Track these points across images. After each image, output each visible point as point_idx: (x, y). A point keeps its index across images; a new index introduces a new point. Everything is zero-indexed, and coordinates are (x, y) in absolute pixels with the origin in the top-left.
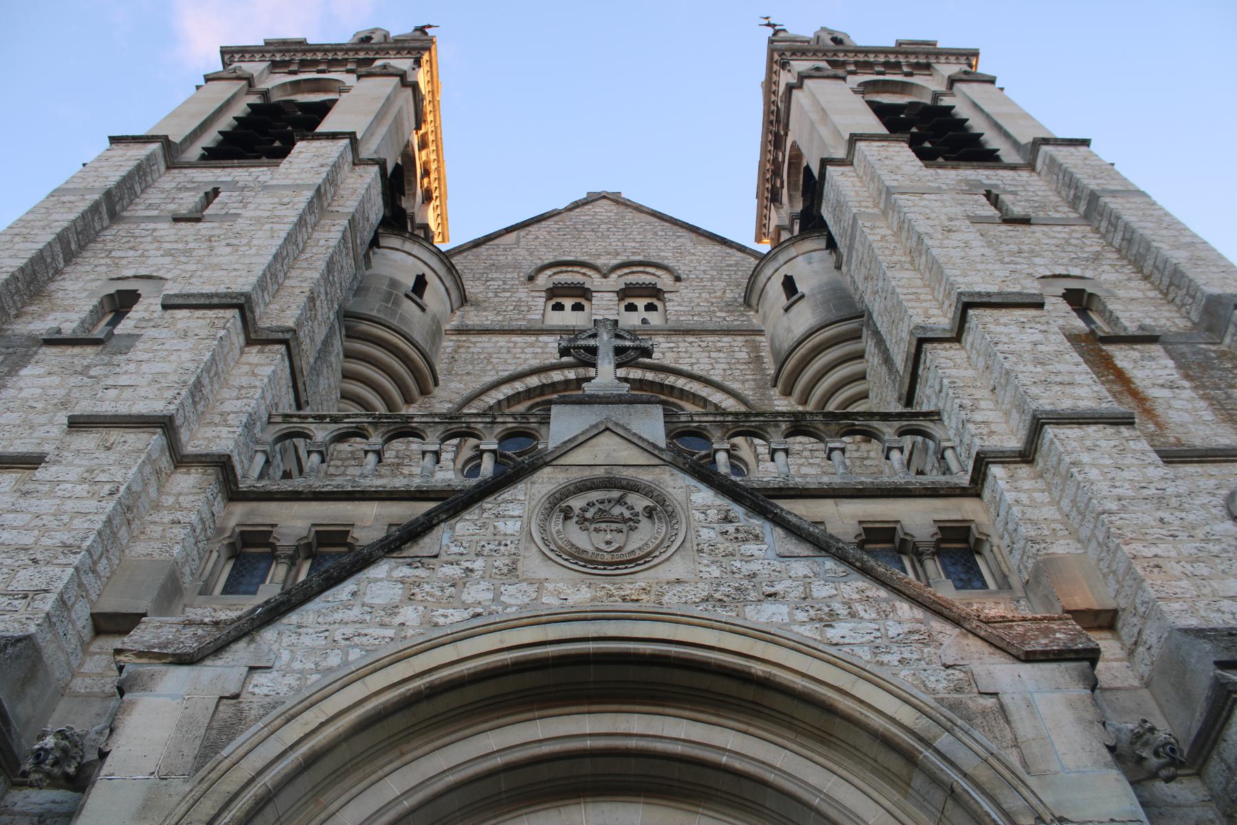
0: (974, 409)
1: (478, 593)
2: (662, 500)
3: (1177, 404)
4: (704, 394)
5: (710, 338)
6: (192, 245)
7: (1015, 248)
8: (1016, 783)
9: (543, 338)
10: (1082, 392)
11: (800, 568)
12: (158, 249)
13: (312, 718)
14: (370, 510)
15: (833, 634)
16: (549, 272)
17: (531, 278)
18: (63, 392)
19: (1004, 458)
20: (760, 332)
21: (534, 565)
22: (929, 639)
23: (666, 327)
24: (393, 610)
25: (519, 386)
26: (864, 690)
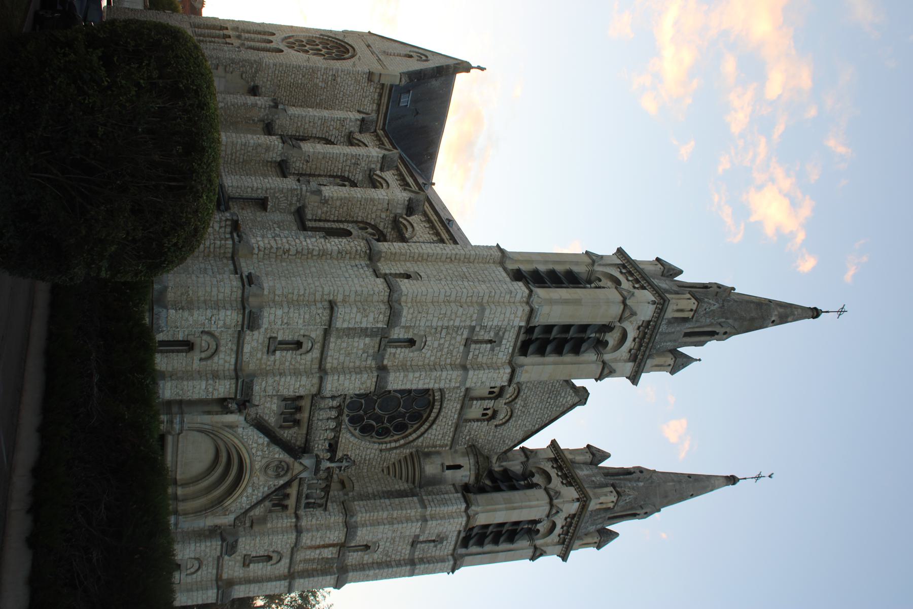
1: (259, 453)
2: (282, 476)
5: (451, 435)
6: (445, 350)
7: (397, 539)
10: (308, 541)
11: (260, 495)
12: (445, 341)
14: (306, 415)
15: (244, 498)
20: (451, 448)
21: (264, 461)
24: (256, 443)
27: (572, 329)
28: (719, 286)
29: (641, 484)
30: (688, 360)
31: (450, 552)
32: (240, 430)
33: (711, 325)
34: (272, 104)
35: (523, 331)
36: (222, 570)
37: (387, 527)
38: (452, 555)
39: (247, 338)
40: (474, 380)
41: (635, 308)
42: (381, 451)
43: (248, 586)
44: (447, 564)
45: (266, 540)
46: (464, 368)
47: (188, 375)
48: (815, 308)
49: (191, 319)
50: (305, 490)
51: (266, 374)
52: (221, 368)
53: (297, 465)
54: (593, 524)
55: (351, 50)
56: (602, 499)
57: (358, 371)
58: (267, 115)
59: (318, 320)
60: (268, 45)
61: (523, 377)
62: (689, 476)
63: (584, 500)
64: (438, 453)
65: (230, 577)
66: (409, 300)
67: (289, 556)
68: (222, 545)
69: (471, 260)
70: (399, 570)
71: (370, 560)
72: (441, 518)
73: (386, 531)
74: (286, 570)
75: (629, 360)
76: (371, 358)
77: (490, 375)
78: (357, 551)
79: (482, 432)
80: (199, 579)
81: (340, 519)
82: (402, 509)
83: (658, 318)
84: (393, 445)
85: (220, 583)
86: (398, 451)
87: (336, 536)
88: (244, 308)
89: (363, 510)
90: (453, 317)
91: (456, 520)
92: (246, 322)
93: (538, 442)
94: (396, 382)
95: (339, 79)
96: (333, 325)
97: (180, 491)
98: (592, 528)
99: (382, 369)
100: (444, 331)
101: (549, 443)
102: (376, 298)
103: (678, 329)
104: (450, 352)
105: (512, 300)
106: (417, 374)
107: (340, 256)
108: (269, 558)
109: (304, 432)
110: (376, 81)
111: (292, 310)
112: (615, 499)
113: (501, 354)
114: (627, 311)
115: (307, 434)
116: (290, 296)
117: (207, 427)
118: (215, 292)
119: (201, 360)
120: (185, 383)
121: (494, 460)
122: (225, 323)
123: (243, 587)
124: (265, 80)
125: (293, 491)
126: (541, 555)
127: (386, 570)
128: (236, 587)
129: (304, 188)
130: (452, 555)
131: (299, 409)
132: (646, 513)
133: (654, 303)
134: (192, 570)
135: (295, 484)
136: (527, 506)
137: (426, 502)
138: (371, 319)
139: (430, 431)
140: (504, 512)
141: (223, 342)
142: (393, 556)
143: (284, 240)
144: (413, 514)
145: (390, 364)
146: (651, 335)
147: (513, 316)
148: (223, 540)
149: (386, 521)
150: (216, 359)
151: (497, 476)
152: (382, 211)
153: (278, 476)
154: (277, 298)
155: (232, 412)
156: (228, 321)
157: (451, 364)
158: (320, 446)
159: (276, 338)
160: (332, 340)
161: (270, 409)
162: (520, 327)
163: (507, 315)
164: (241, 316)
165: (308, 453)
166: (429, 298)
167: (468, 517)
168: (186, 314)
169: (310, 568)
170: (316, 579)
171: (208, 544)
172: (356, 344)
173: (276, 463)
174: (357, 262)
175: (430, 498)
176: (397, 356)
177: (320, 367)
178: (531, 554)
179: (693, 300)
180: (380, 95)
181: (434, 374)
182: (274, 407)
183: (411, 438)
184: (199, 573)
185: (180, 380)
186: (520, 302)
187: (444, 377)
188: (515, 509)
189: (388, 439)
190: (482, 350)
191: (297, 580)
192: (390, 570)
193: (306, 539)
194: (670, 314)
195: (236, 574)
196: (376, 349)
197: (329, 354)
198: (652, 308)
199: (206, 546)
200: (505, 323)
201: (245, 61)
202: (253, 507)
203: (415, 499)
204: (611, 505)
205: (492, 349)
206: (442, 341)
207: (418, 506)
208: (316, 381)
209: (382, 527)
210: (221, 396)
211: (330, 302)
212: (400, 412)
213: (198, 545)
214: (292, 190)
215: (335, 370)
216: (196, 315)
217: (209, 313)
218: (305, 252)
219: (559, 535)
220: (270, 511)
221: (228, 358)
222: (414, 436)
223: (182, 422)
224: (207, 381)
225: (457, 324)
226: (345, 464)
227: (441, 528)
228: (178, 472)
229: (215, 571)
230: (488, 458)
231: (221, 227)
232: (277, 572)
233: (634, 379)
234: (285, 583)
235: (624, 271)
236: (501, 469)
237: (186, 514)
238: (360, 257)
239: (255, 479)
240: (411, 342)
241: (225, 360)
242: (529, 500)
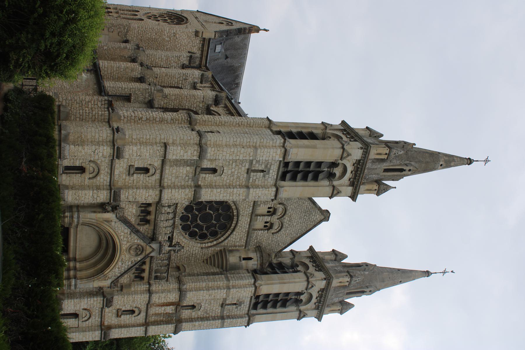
0: (162, 287)
1: (125, 239)
2: (139, 255)
3: (160, 310)
5: (245, 239)
6: (236, 176)
7: (212, 302)
8: (97, 279)
9: (251, 208)
10: (157, 300)
11: (126, 267)
13: (109, 228)
15: (117, 269)
17: (280, 204)
18: (181, 175)
19: (149, 287)
20: (245, 248)
21: (128, 244)
22: (115, 276)
23: (251, 230)
26: (109, 270)
27: (312, 164)
28: (405, 143)
29: (367, 273)
30: (387, 188)
31: (246, 312)
32: (113, 223)
33: (400, 165)
34: (136, 47)
35: (282, 165)
36: (104, 319)
37: (205, 292)
38: (248, 314)
39: (117, 165)
40: (254, 195)
41: (350, 151)
42: (202, 248)
43: (120, 329)
44: (244, 319)
45: (131, 298)
46: (248, 187)
47: (82, 187)
48: (469, 159)
49: (83, 151)
50: (154, 267)
51: (128, 187)
52: (102, 184)
53: (148, 247)
54: (336, 297)
55: (185, 20)
56: (341, 280)
57: (183, 187)
58: (133, 54)
59: (158, 154)
60: (135, 17)
61: (284, 194)
62: (399, 270)
63: (329, 279)
64: (238, 250)
65: (109, 324)
66: (212, 144)
67: (145, 311)
68: (103, 300)
69: (251, 125)
70: (214, 322)
71: (196, 316)
72: (239, 288)
73: (205, 295)
74: (144, 321)
75: (350, 185)
76: (191, 180)
77: (263, 192)
78: (188, 309)
79: (263, 237)
80: (90, 325)
81: (176, 286)
82: (214, 281)
83: (365, 158)
84: (210, 244)
85: (103, 327)
86: (213, 249)
87: (173, 297)
88: (114, 146)
89: (190, 281)
90: (239, 154)
91: (248, 289)
92: (115, 154)
93: (301, 246)
94: (206, 195)
95: (178, 36)
96: (167, 157)
97: (78, 265)
98: (336, 300)
99: (198, 187)
100: (234, 164)
101: (308, 248)
102: (192, 142)
103: (379, 166)
104: (238, 177)
105: (274, 145)
106: (219, 190)
107: (172, 121)
108: (132, 312)
109: (152, 228)
110: (200, 36)
111: (142, 147)
112: (349, 280)
113: (270, 180)
114: (345, 154)
115: (154, 229)
116: (141, 139)
117: (93, 221)
118: (97, 136)
119: (90, 178)
120: (80, 192)
121: (273, 257)
122: (103, 155)
123: (117, 330)
124: (133, 36)
125: (146, 267)
126: (304, 316)
127: (206, 322)
128: (113, 330)
129: (153, 88)
130: (248, 314)
131: (149, 213)
132: (370, 291)
133: (362, 148)
134: (86, 318)
135: (148, 260)
136: (293, 283)
137: (230, 278)
138: (189, 153)
139: (232, 236)
140: (278, 286)
141: (102, 168)
142: (211, 314)
143: (139, 113)
144: (221, 285)
145: (202, 184)
146: (362, 169)
147: (275, 154)
148: (104, 297)
149: (205, 289)
150: (98, 178)
151: (274, 265)
152: (200, 102)
153: (137, 255)
154: (134, 140)
155: (108, 212)
156: (105, 153)
157: (239, 185)
158: (162, 237)
159: (133, 166)
160: (167, 168)
161: (131, 212)
162: (280, 161)
163: (271, 153)
164: (112, 150)
165: (156, 240)
166: (224, 143)
167: (256, 287)
168: (80, 148)
169: (159, 319)
170: (162, 326)
171: (95, 299)
172: (181, 171)
173: (135, 246)
174: (182, 125)
175: (232, 276)
176: (206, 179)
177: (160, 185)
178: (298, 315)
179: (387, 148)
180: (203, 45)
181: (229, 190)
182: (134, 211)
183: (220, 240)
184: (90, 320)
185: (76, 192)
186: (279, 146)
188: (285, 283)
189: (206, 241)
190: (258, 177)
191: (151, 327)
192: (209, 322)
193: (155, 299)
194: (373, 155)
195: (113, 322)
196: (193, 175)
197: (166, 177)
198: (361, 151)
199: (94, 301)
200: (270, 158)
201: (121, 25)
202: (122, 275)
203: (223, 276)
204: (347, 284)
205: (264, 176)
206: (233, 170)
207: (224, 279)
208: (158, 192)
209: (202, 292)
210: (102, 201)
211: (165, 143)
212: (213, 223)
213: (89, 299)
214: (145, 89)
215: (169, 187)
216: (86, 150)
217: (94, 148)
218: (152, 119)
219: (315, 304)
220: (134, 281)
221: (105, 178)
222: (222, 239)
223: (78, 217)
224: (93, 190)
225: (241, 158)
226: (177, 248)
227: (240, 294)
228: (77, 254)
229: (99, 320)
230: (269, 255)
231: (102, 105)
232: (138, 322)
233: (354, 197)
234: (143, 329)
235: (345, 133)
236: (277, 262)
237: (81, 279)
238: (184, 122)
239: (123, 256)
240: (214, 171)
241: (103, 178)
242: (294, 279)
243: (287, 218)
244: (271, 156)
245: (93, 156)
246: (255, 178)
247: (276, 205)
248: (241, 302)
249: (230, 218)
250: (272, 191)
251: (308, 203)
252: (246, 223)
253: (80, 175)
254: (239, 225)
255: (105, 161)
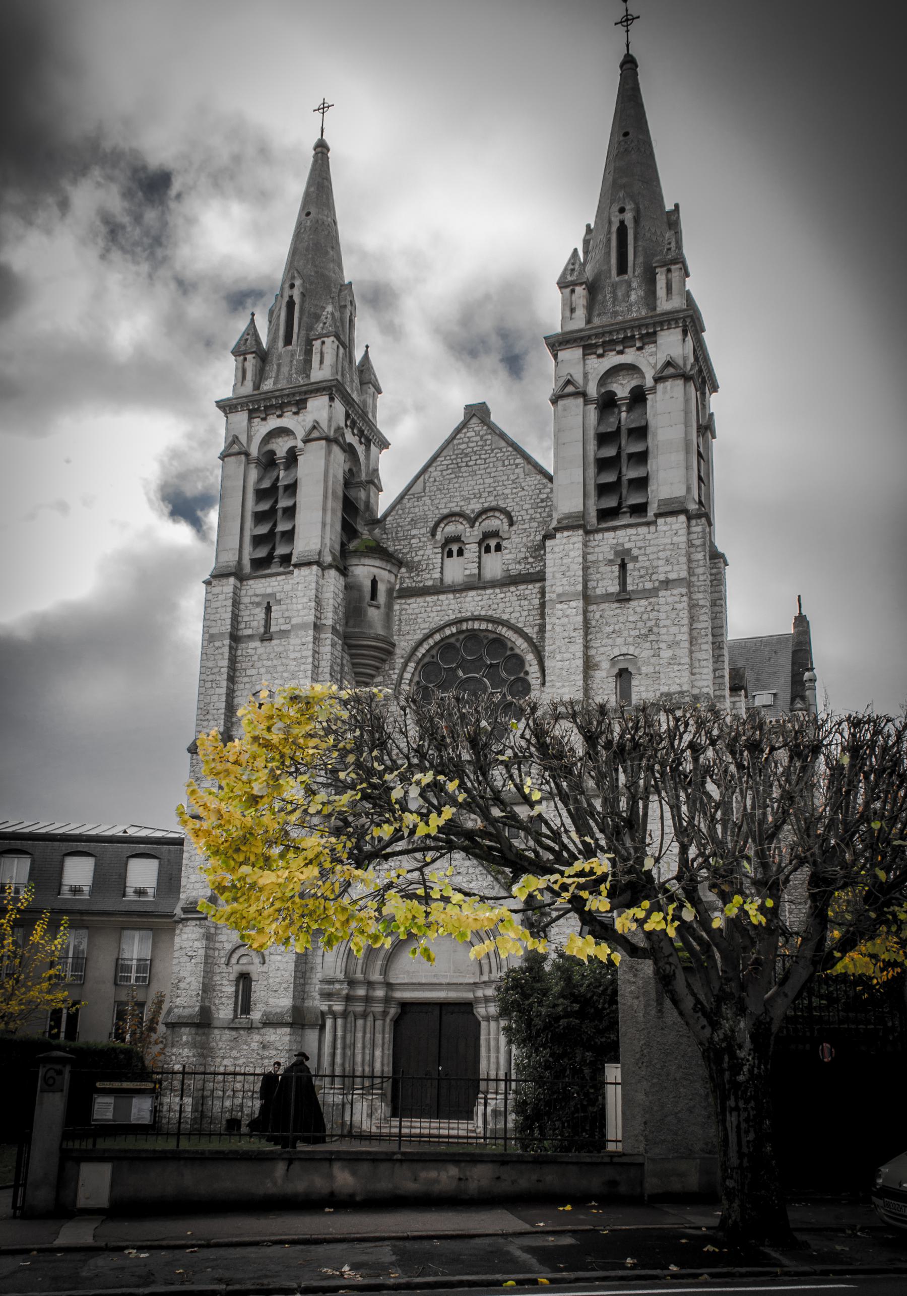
4: (513, 640)
6: (275, 662)
7: (610, 629)
9: (442, 597)
11: (467, 863)
15: (471, 885)
16: (442, 525)
17: (433, 534)
25: (431, 642)
49: (187, 980)
77: (300, 594)
156: (194, 936)
187: (298, 655)
189: (529, 678)
190: (279, 615)
205: (279, 602)
206: (263, 670)
243: (471, 507)
244: (225, 603)
245: (198, 960)
246: (282, 621)
247: (436, 542)
248: (617, 553)
249: (473, 635)
250: (298, 577)
251: (434, 472)
252: (480, 598)
253: (253, 983)
254: (483, 613)
255: (227, 934)
